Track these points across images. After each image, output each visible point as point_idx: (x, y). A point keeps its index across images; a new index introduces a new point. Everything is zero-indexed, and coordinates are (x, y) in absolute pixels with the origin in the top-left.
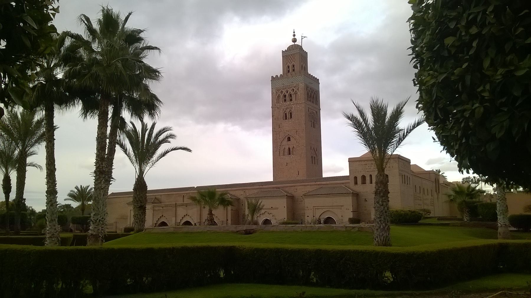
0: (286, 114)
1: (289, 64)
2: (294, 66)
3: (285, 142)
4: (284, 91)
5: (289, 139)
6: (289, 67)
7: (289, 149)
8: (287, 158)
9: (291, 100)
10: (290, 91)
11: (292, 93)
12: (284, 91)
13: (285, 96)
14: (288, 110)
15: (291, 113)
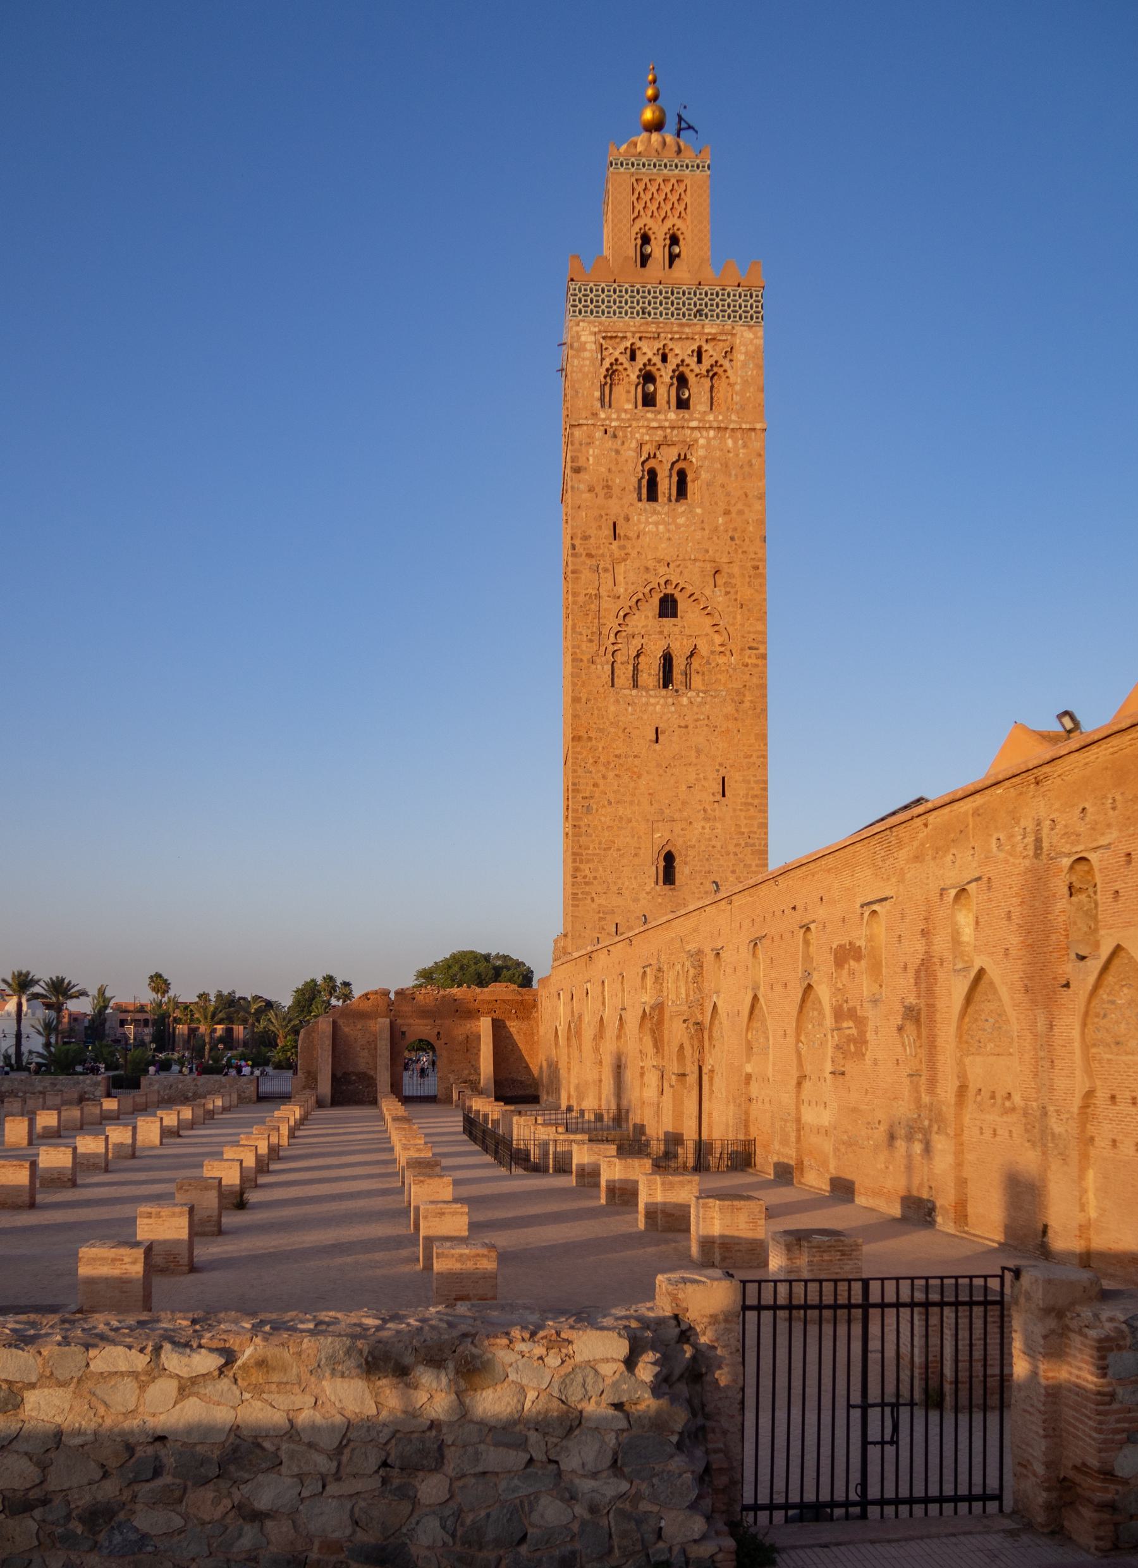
0: (652, 473)
1: (650, 223)
2: (674, 240)
3: (646, 618)
4: (648, 351)
5: (668, 607)
6: (646, 239)
7: (667, 660)
8: (657, 704)
9: (683, 404)
10: (681, 351)
11: (694, 366)
12: (648, 351)
13: (648, 377)
14: (669, 455)
15: (682, 475)
